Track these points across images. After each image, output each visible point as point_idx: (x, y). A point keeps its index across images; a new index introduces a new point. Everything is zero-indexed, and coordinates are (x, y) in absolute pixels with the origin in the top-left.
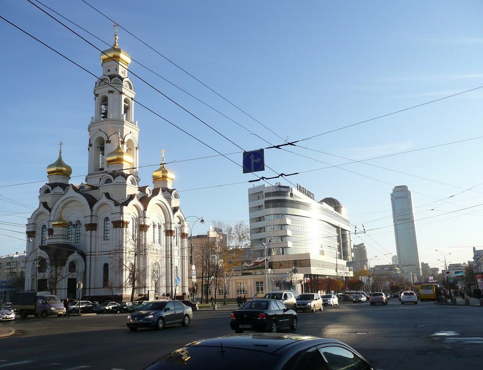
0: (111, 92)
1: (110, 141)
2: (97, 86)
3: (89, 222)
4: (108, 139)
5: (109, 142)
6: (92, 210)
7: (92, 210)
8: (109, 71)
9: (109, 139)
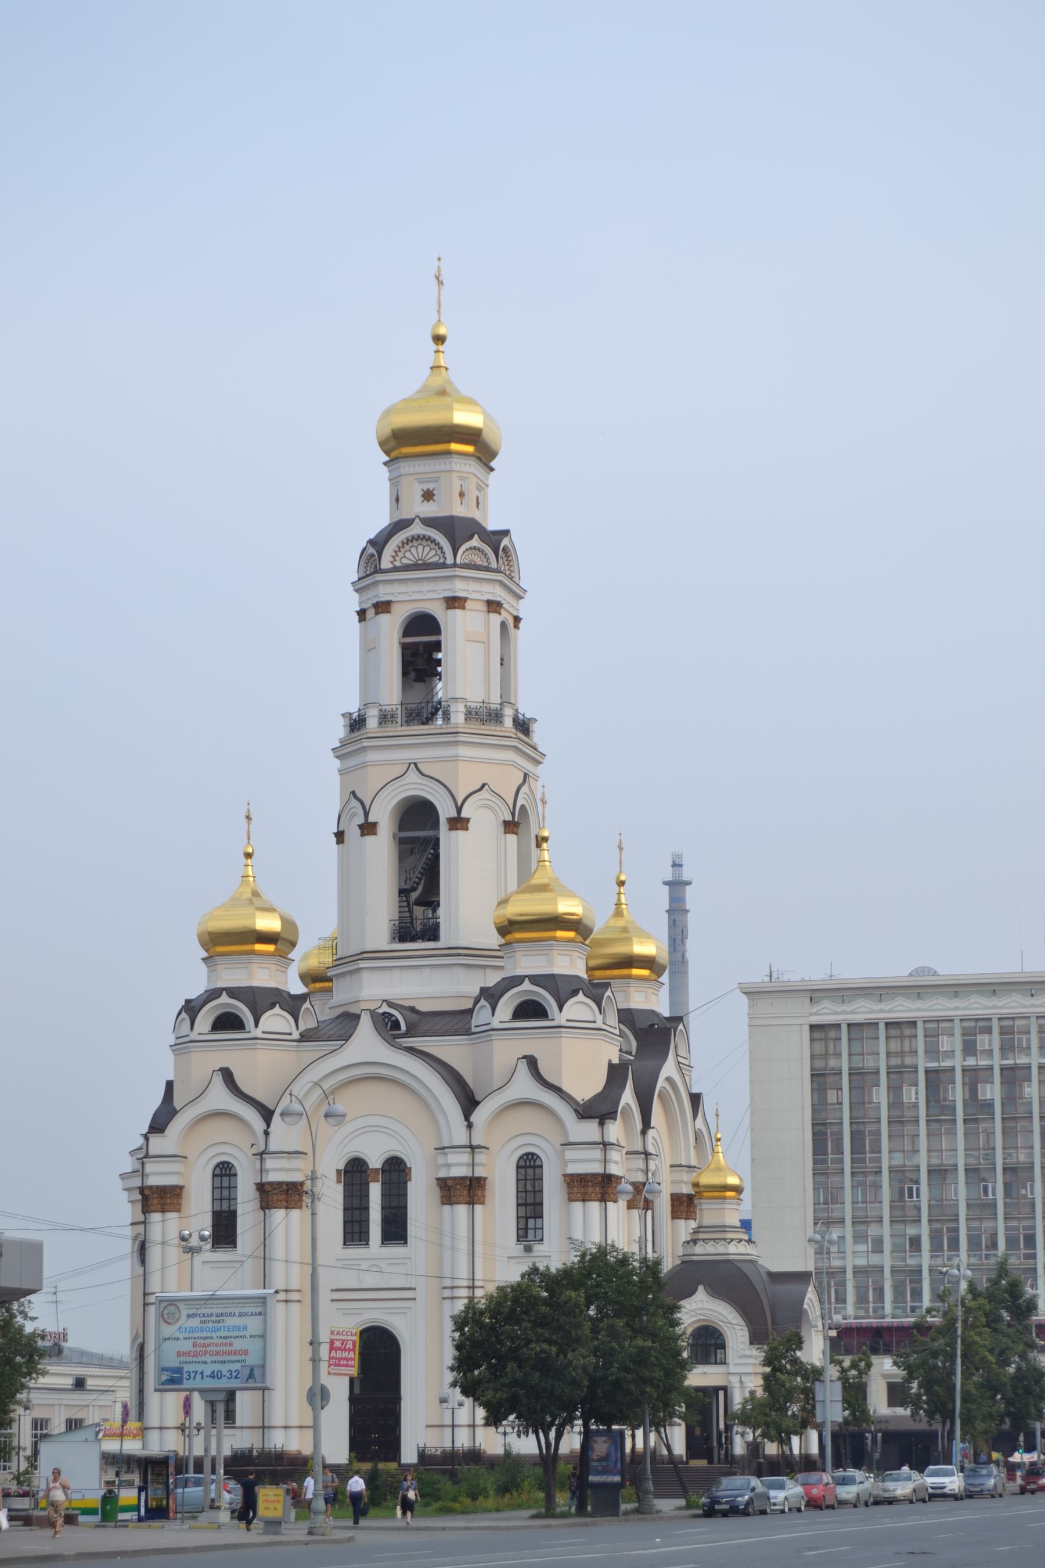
0: (454, 602)
1: (468, 820)
2: (386, 563)
3: (460, 1171)
4: (459, 810)
5: (459, 823)
6: (470, 1126)
7: (470, 1126)
8: (428, 496)
9: (464, 815)
